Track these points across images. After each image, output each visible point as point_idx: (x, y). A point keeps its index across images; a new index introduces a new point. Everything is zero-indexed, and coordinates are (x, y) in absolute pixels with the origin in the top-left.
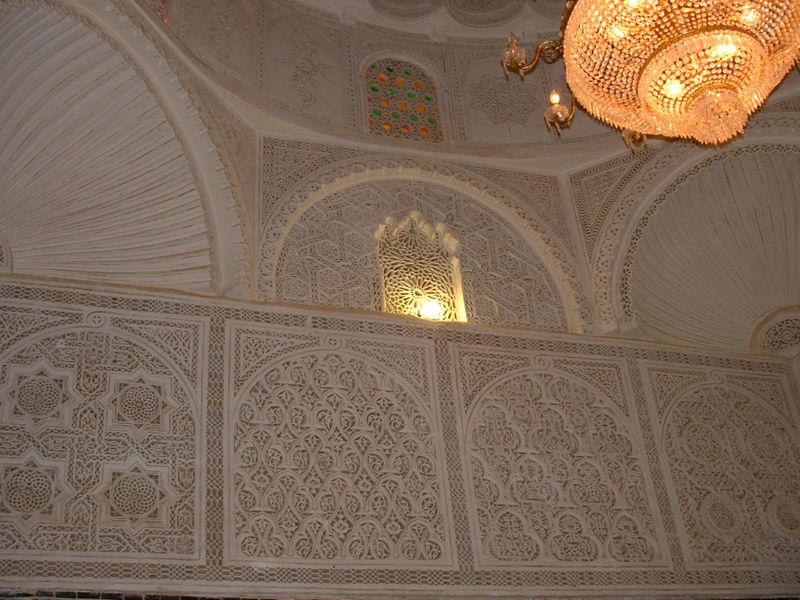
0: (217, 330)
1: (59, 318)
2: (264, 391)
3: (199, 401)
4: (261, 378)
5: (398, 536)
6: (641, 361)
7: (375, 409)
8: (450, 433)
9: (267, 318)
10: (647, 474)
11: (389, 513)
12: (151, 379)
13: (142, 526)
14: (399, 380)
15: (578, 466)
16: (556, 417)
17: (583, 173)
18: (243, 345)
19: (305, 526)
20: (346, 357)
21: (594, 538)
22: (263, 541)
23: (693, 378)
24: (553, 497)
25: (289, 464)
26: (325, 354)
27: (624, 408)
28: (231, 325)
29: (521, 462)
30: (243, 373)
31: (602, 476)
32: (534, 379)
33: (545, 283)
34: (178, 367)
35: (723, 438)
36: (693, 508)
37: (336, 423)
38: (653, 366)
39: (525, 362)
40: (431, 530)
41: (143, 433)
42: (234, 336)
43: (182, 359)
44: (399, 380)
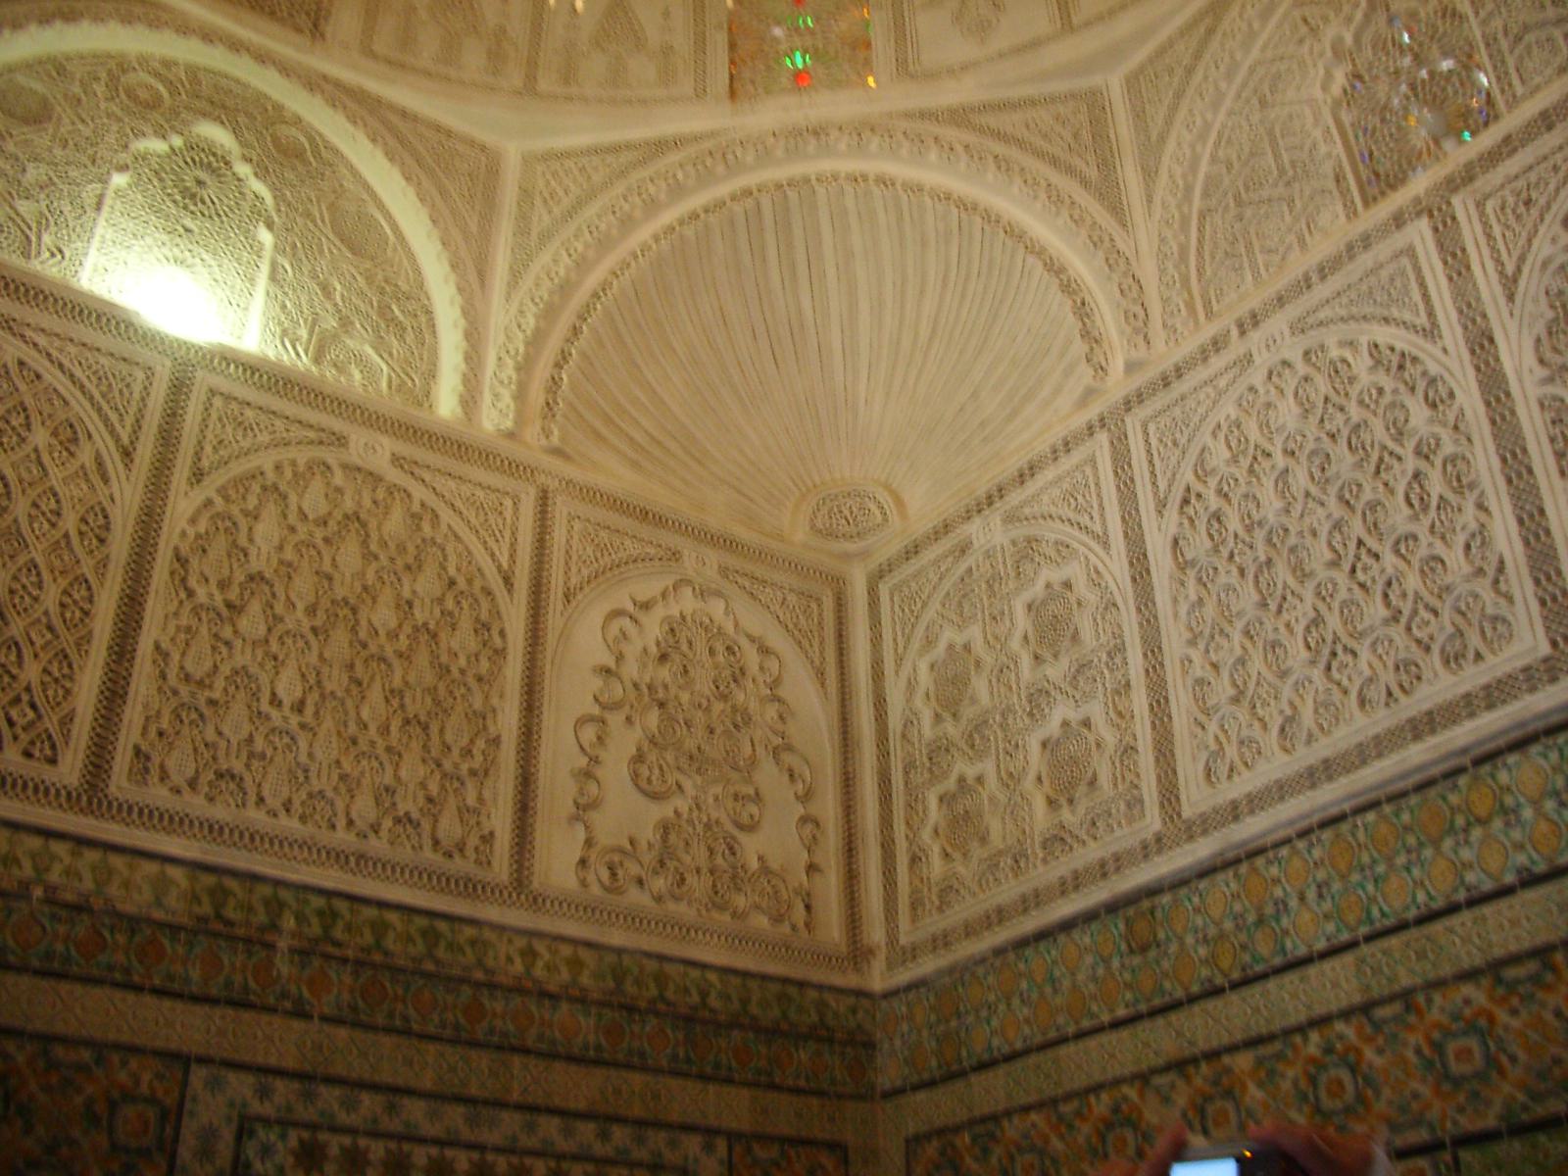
7: (1355, 413)
14: (1383, 335)
22: (1231, 752)
40: (1487, 595)
41: (1064, 662)
43: (1085, 520)
44: (1383, 335)
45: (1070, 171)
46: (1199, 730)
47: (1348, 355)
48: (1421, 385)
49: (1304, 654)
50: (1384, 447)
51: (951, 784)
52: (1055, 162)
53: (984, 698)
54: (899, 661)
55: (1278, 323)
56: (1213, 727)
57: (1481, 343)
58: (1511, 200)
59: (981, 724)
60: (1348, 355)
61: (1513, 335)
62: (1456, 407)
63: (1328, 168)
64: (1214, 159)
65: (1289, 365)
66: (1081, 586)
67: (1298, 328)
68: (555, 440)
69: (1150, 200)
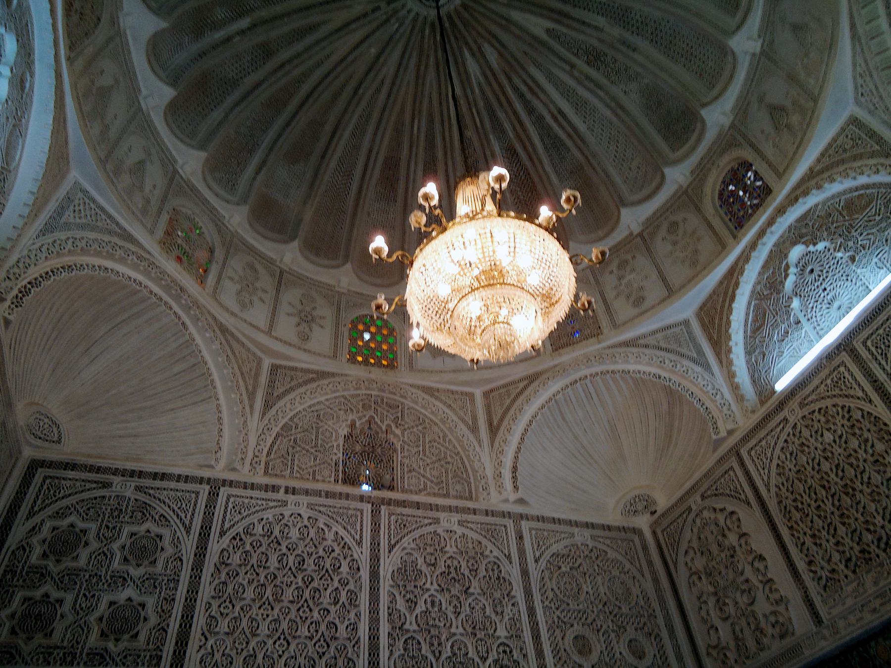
0: (213, 495)
1: (94, 485)
2: (241, 540)
3: (189, 545)
4: (241, 530)
5: (324, 654)
6: (524, 523)
7: (321, 553)
8: (374, 575)
9: (253, 487)
10: (523, 607)
11: (320, 634)
12: (155, 529)
13: (122, 645)
14: (342, 532)
15: (470, 600)
16: (455, 563)
17: (492, 391)
18: (231, 506)
19: (253, 644)
20: (305, 516)
21: (477, 659)
24: (448, 625)
25: (249, 594)
26: (290, 513)
27: (509, 557)
28: (224, 492)
29: (426, 596)
30: (227, 526)
31: (488, 610)
32: (442, 534)
33: (460, 465)
34: (178, 522)
35: (586, 582)
36: (559, 638)
37: (291, 563)
39: (437, 521)
40: (350, 650)
41: (141, 571)
42: (225, 498)
43: (183, 516)
44: (342, 532)
45: (244, 381)
46: (203, 639)
47: (326, 529)
48: (349, 559)
49: (267, 632)
50: (327, 571)
51: (38, 594)
52: (242, 374)
53: (82, 562)
54: (31, 514)
55: (304, 499)
56: (211, 642)
57: (375, 559)
58: (400, 521)
59: (74, 573)
60: (326, 529)
61: (387, 565)
62: (358, 576)
63: (335, 457)
64: (291, 419)
65: (301, 516)
66: (166, 542)
67: (310, 506)
68: (11, 317)
69: (264, 414)
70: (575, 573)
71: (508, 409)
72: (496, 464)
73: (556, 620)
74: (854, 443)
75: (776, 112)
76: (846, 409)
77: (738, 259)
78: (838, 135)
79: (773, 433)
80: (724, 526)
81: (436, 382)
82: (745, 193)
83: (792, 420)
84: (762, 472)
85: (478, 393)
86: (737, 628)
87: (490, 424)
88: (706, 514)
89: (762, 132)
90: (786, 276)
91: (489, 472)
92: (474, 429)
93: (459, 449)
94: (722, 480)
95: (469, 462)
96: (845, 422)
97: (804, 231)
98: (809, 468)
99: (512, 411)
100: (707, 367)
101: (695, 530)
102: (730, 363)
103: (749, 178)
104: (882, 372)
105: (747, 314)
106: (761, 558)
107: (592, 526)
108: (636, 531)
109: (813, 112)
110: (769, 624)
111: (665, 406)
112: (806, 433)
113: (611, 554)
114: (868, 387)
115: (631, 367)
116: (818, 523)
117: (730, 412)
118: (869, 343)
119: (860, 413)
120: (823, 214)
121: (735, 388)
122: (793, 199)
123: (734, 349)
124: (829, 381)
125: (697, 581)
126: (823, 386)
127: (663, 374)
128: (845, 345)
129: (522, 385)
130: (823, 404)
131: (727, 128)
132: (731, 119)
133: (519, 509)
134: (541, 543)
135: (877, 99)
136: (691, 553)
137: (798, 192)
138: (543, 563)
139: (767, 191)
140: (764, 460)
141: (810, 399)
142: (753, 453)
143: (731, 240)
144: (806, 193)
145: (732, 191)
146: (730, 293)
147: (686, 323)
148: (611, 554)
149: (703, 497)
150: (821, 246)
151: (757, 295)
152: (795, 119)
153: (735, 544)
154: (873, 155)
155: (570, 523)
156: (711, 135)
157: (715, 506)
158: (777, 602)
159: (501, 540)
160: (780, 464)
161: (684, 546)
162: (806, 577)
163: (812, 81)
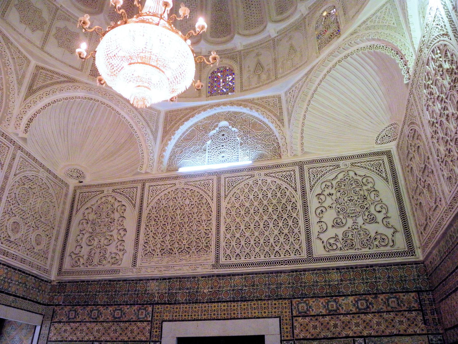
6: (19, 151)
17: (43, 68)
23: (34, 169)
35: (33, 198)
38: (23, 156)
70: (30, 191)
71: (47, 86)
72: (22, 111)
73: (9, 210)
74: (195, 210)
75: (259, 65)
76: (201, 197)
77: (202, 106)
78: (272, 97)
79: (166, 186)
80: (116, 209)
81: (14, 38)
82: (223, 82)
83: (177, 186)
84: (150, 197)
85: (33, 63)
86: (93, 252)
87: (30, 87)
88: (110, 199)
89: (249, 67)
90: (214, 129)
91: (16, 112)
92: (20, 83)
93: (4, 87)
94: (129, 190)
95: (6, 101)
96: (198, 201)
97: (233, 118)
98: (171, 209)
99: (48, 89)
100: (155, 139)
101: (99, 202)
102: (166, 145)
103: (229, 78)
104: (224, 192)
105: (187, 130)
106: (125, 230)
107: (49, 171)
108: (67, 185)
109: (272, 81)
110: (110, 257)
111: (123, 141)
112: (180, 195)
113: (51, 191)
114: (215, 194)
115: (123, 113)
116: (160, 230)
117: (152, 165)
118: (227, 179)
119: (205, 201)
120: (244, 118)
121: (161, 156)
122: (239, 104)
123: (172, 140)
124: (202, 182)
125: (84, 223)
126: (199, 182)
127: (135, 127)
128: (218, 174)
129: (62, 79)
130: (194, 189)
131: (237, 50)
132: (242, 48)
133: (21, 143)
134: (22, 167)
135: (293, 100)
136: (90, 210)
137: (243, 103)
138: (17, 178)
139: (232, 90)
140: (154, 194)
141: (191, 183)
142: (151, 188)
143: (204, 95)
144: (245, 106)
145: (218, 76)
146: (188, 116)
147: (159, 112)
148: (51, 191)
149: (113, 191)
150: (234, 129)
151: (196, 126)
152: (264, 77)
153: (116, 219)
154: (275, 115)
155: (41, 165)
156: (229, 46)
157: (117, 198)
158: (120, 250)
159: (3, 154)
160: (160, 199)
161: (88, 205)
162: (141, 247)
163: (281, 70)
